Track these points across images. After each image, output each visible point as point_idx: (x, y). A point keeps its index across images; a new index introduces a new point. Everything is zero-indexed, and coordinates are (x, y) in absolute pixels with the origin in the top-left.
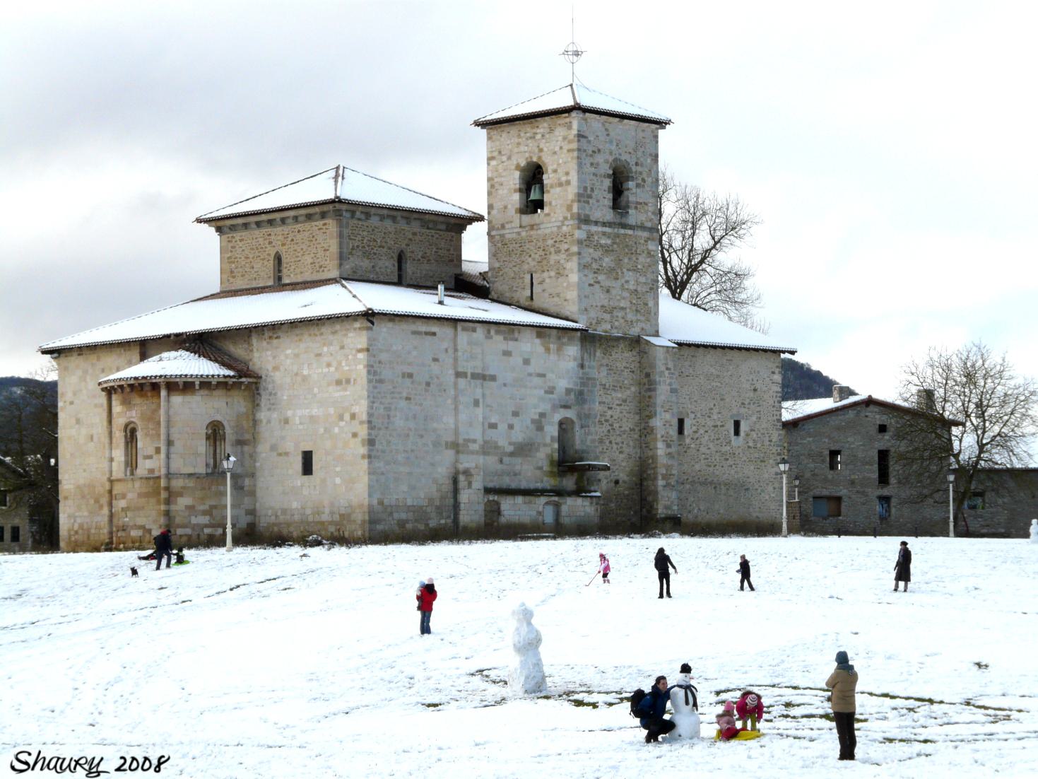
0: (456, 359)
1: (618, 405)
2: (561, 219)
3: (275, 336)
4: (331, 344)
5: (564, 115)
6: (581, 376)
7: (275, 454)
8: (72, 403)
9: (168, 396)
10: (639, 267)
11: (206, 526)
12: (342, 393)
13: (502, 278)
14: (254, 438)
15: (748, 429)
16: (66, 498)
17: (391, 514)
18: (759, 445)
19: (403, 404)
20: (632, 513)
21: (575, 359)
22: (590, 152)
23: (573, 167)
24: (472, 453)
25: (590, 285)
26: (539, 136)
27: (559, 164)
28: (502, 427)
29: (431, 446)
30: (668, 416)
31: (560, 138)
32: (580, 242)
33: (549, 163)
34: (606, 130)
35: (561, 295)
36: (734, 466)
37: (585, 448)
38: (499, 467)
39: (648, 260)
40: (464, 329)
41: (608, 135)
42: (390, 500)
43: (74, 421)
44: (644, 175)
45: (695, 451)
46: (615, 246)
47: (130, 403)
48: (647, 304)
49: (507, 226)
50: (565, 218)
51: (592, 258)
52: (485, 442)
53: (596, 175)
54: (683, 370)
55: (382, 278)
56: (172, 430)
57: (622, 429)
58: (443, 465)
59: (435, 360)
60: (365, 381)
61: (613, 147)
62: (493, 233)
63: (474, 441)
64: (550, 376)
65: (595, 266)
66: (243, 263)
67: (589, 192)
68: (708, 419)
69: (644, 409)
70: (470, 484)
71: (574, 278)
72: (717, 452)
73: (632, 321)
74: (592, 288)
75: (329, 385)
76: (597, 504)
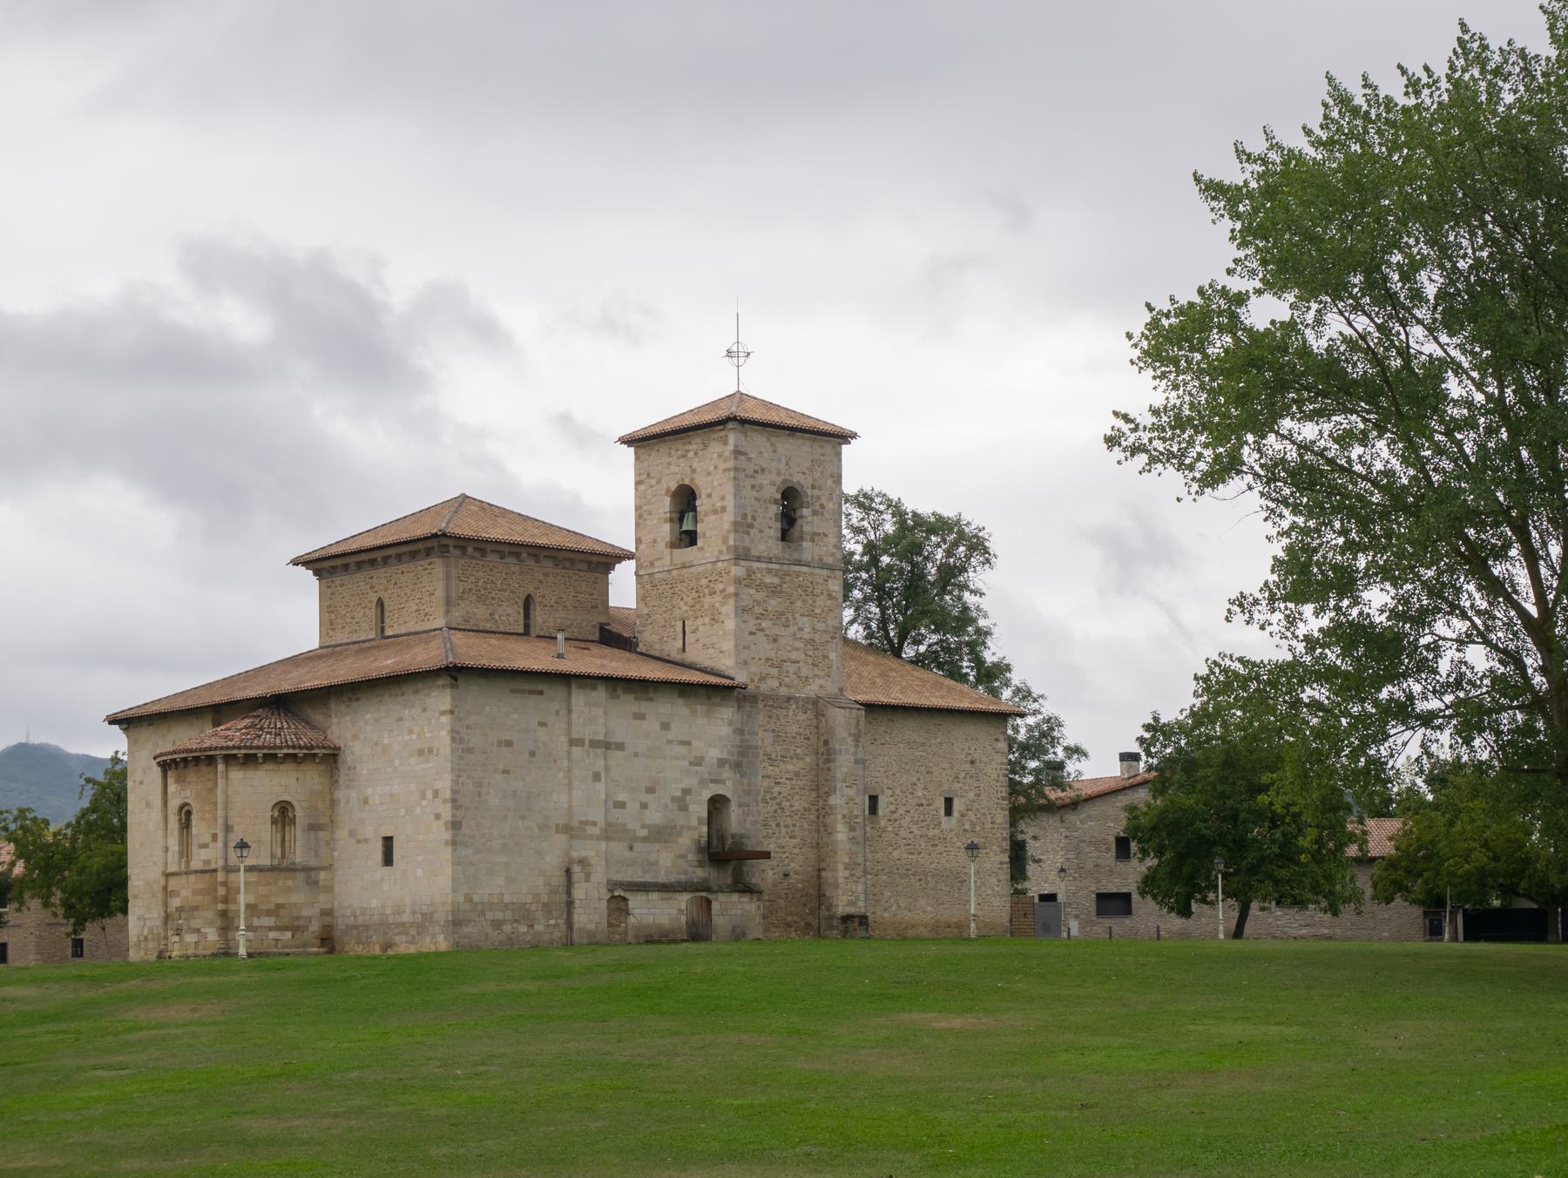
0: (569, 723)
1: (787, 779)
2: (716, 553)
3: (354, 697)
4: (413, 706)
5: (719, 428)
6: (738, 743)
7: (353, 841)
8: (141, 783)
9: (226, 768)
10: (817, 611)
11: (270, 929)
13: (650, 627)
14: (331, 821)
15: (963, 808)
16: (135, 897)
17: (482, 913)
18: (978, 828)
19: (499, 777)
20: (807, 911)
21: (730, 723)
22: (752, 473)
23: (728, 489)
24: (591, 837)
25: (751, 633)
26: (691, 454)
27: (713, 487)
28: (632, 807)
29: (537, 830)
30: (851, 792)
31: (715, 456)
32: (738, 581)
33: (703, 486)
34: (773, 445)
35: (716, 646)
36: (945, 854)
37: (743, 832)
38: (628, 854)
39: (829, 603)
40: (580, 687)
41: (775, 451)
42: (483, 893)
43: (143, 803)
44: (824, 501)
45: (892, 835)
46: (785, 586)
47: (184, 781)
48: (827, 657)
49: (656, 564)
50: (721, 552)
51: (754, 601)
52: (609, 825)
53: (759, 500)
54: (877, 736)
55: (502, 628)
56: (231, 813)
57: (794, 809)
58: (554, 852)
59: (542, 724)
60: (448, 750)
61: (782, 466)
62: (641, 573)
63: (594, 824)
64: (696, 744)
65: (757, 610)
66: (344, 612)
67: (749, 519)
68: (910, 796)
69: (821, 782)
70: (588, 878)
71: (730, 624)
72: (921, 836)
73: (807, 677)
74: (752, 637)
75: (411, 756)
76: (759, 900)
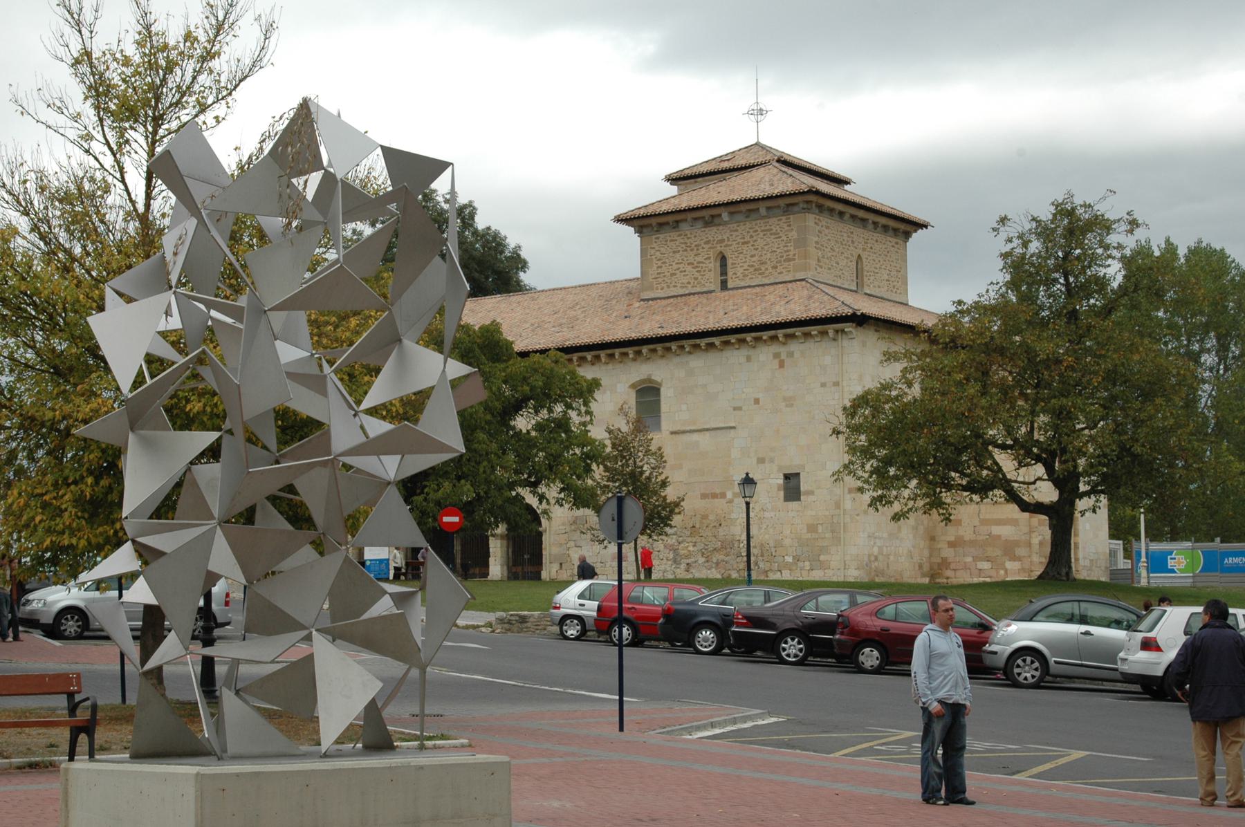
66: (829, 254)
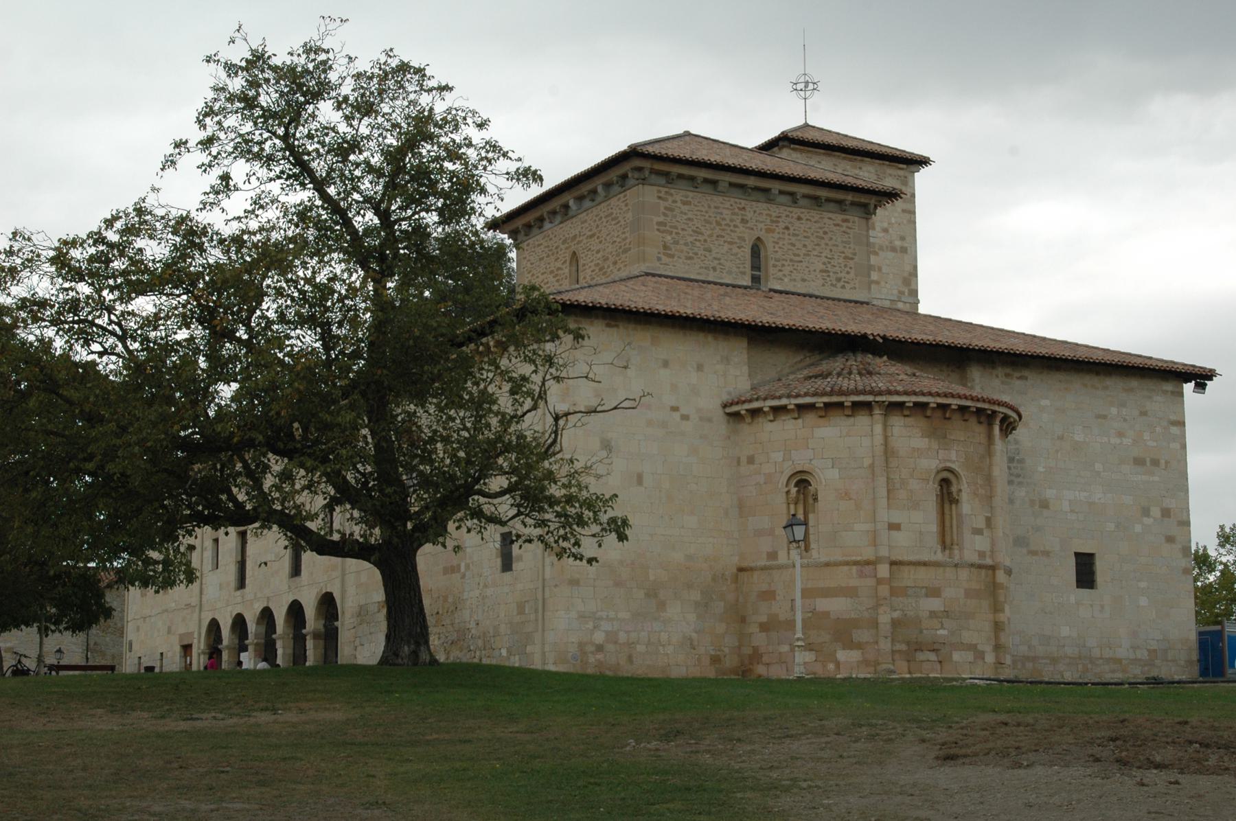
3: (1017, 374)
5: (901, 166)
12: (1145, 478)
47: (945, 437)
50: (901, 293)
66: (690, 239)
